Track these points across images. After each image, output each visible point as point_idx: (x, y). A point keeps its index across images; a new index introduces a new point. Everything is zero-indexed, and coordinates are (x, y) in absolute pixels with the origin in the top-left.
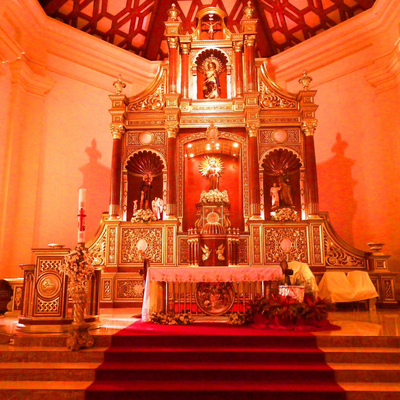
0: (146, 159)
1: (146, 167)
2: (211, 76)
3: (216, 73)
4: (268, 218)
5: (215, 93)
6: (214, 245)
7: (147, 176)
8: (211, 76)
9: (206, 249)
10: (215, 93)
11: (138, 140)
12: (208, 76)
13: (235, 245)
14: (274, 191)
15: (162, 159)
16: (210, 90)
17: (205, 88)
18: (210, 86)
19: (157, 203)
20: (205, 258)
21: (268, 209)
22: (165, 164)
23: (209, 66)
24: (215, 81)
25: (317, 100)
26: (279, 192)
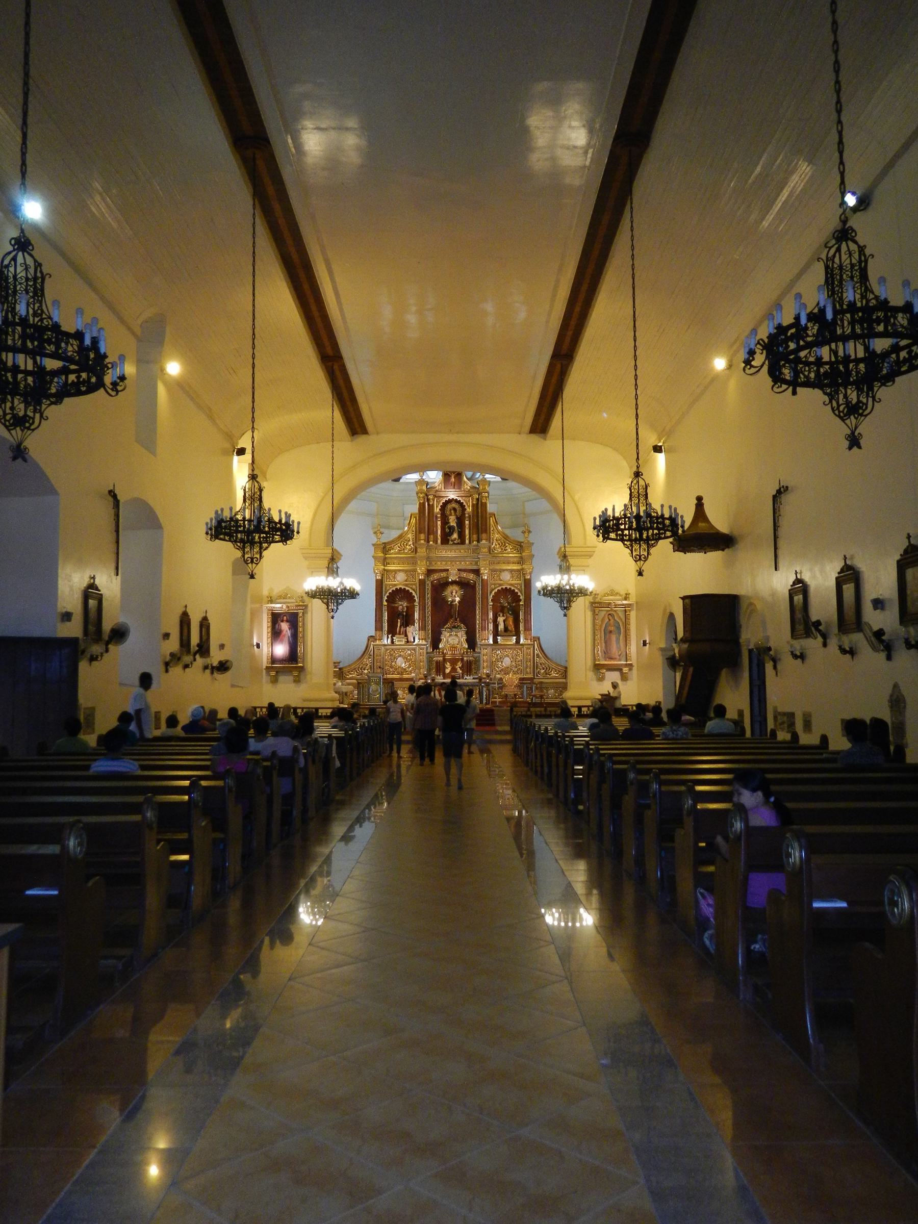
0: (401, 593)
1: (401, 599)
3: (457, 518)
4: (495, 641)
5: (455, 536)
6: (453, 662)
7: (402, 605)
8: (453, 522)
9: (448, 665)
10: (455, 536)
11: (394, 578)
13: (469, 664)
14: (501, 620)
16: (451, 534)
17: (447, 530)
18: (451, 528)
19: (410, 629)
20: (448, 671)
21: (496, 634)
25: (534, 550)
26: (504, 621)
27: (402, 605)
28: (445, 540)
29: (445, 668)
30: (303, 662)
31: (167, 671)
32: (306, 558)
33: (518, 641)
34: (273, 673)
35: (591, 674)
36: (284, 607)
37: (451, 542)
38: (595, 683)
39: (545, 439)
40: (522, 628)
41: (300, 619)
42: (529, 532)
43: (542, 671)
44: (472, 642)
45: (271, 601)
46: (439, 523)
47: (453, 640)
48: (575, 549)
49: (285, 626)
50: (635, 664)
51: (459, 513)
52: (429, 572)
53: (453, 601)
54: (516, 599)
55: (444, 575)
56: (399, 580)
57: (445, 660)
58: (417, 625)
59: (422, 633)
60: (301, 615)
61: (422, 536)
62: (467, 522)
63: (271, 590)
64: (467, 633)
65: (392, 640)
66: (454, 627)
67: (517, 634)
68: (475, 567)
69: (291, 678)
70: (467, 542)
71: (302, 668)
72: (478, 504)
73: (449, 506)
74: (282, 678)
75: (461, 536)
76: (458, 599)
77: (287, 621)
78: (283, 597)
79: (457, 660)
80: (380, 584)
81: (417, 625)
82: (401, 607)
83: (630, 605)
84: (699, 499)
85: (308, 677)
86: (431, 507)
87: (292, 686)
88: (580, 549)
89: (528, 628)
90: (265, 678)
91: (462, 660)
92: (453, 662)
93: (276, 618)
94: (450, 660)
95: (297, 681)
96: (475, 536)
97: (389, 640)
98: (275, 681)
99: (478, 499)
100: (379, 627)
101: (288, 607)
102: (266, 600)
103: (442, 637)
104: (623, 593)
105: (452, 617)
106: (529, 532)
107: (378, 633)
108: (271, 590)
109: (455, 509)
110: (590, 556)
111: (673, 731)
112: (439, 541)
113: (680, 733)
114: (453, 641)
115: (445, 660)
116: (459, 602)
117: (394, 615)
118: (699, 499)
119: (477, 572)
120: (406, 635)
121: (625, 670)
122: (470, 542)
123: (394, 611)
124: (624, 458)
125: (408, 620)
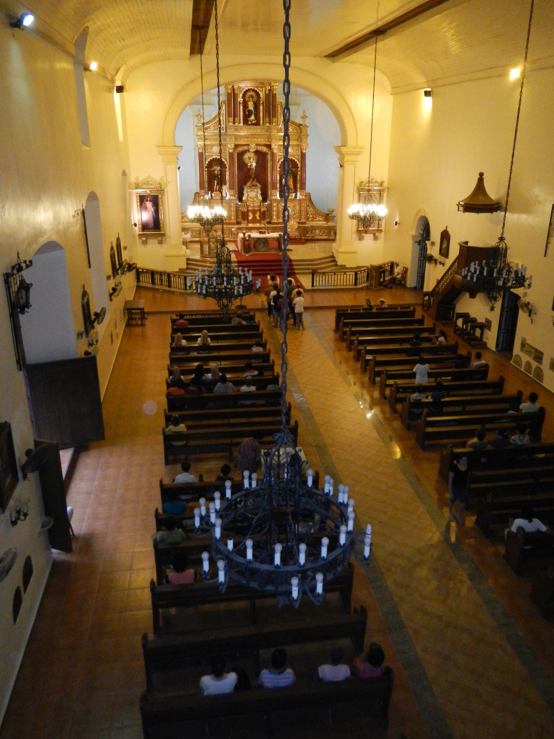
1: (216, 165)
2: (251, 106)
5: (253, 117)
6: (254, 212)
7: (217, 169)
8: (251, 106)
10: (253, 117)
12: (249, 106)
13: (264, 212)
15: (225, 162)
16: (250, 116)
17: (247, 113)
18: (250, 111)
20: (250, 218)
22: (227, 165)
23: (249, 98)
24: (253, 109)
27: (217, 169)
28: (246, 122)
29: (248, 216)
30: (164, 231)
31: (111, 300)
32: (160, 154)
33: (296, 197)
34: (144, 239)
35: (355, 236)
36: (148, 191)
37: (250, 123)
38: (357, 242)
39: (333, 62)
40: (298, 186)
41: (160, 200)
42: (307, 117)
43: (311, 216)
44: (265, 197)
45: (137, 187)
46: (241, 107)
47: (253, 195)
48: (350, 150)
49: (149, 204)
50: (383, 230)
51: (255, 99)
52: (236, 146)
53: (252, 165)
54: (296, 166)
55: (245, 148)
56: (214, 152)
57: (248, 210)
58: (228, 184)
59: (232, 192)
60: (160, 197)
61: (231, 119)
62: (261, 107)
63: (137, 178)
64: (261, 189)
65: (211, 195)
66: (253, 185)
67: (296, 192)
68: (268, 143)
69: (156, 241)
70: (261, 122)
71: (163, 235)
72: (269, 94)
73: (249, 94)
74: (150, 241)
75: (257, 117)
76: (254, 164)
77: (150, 201)
78: (147, 183)
79: (257, 211)
80: (201, 155)
81: (228, 184)
82: (216, 172)
83: (383, 190)
84: (481, 175)
85: (168, 240)
86: (235, 96)
87: (158, 245)
88: (353, 150)
89: (303, 187)
90: (138, 241)
91: (260, 210)
92: (254, 212)
93: (142, 199)
94: (251, 211)
95: (161, 242)
96: (267, 119)
97: (210, 195)
98: (145, 243)
99: (270, 90)
100: (202, 187)
101: (150, 191)
102: (134, 186)
103: (245, 192)
104: (379, 181)
105: (250, 178)
106: (307, 117)
107: (203, 191)
108: (137, 178)
109: (252, 96)
110: (360, 154)
111: (520, 440)
112: (242, 121)
113: (524, 441)
114: (252, 194)
115: (248, 210)
116: (255, 167)
117: (212, 177)
118: (481, 175)
119: (269, 146)
120: (221, 193)
121: (377, 234)
122: (263, 123)
123: (212, 177)
124: (389, 79)
125: (222, 182)
